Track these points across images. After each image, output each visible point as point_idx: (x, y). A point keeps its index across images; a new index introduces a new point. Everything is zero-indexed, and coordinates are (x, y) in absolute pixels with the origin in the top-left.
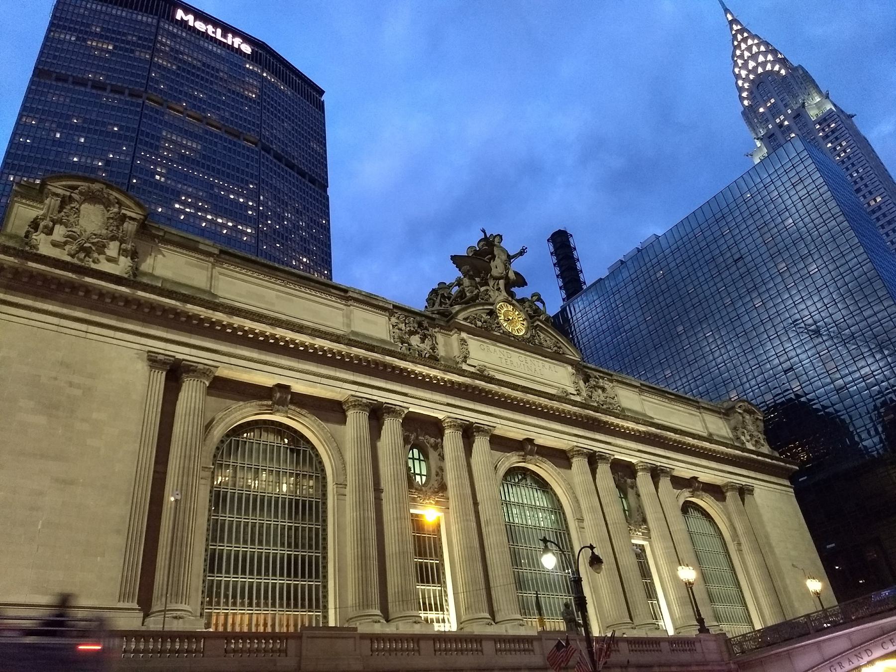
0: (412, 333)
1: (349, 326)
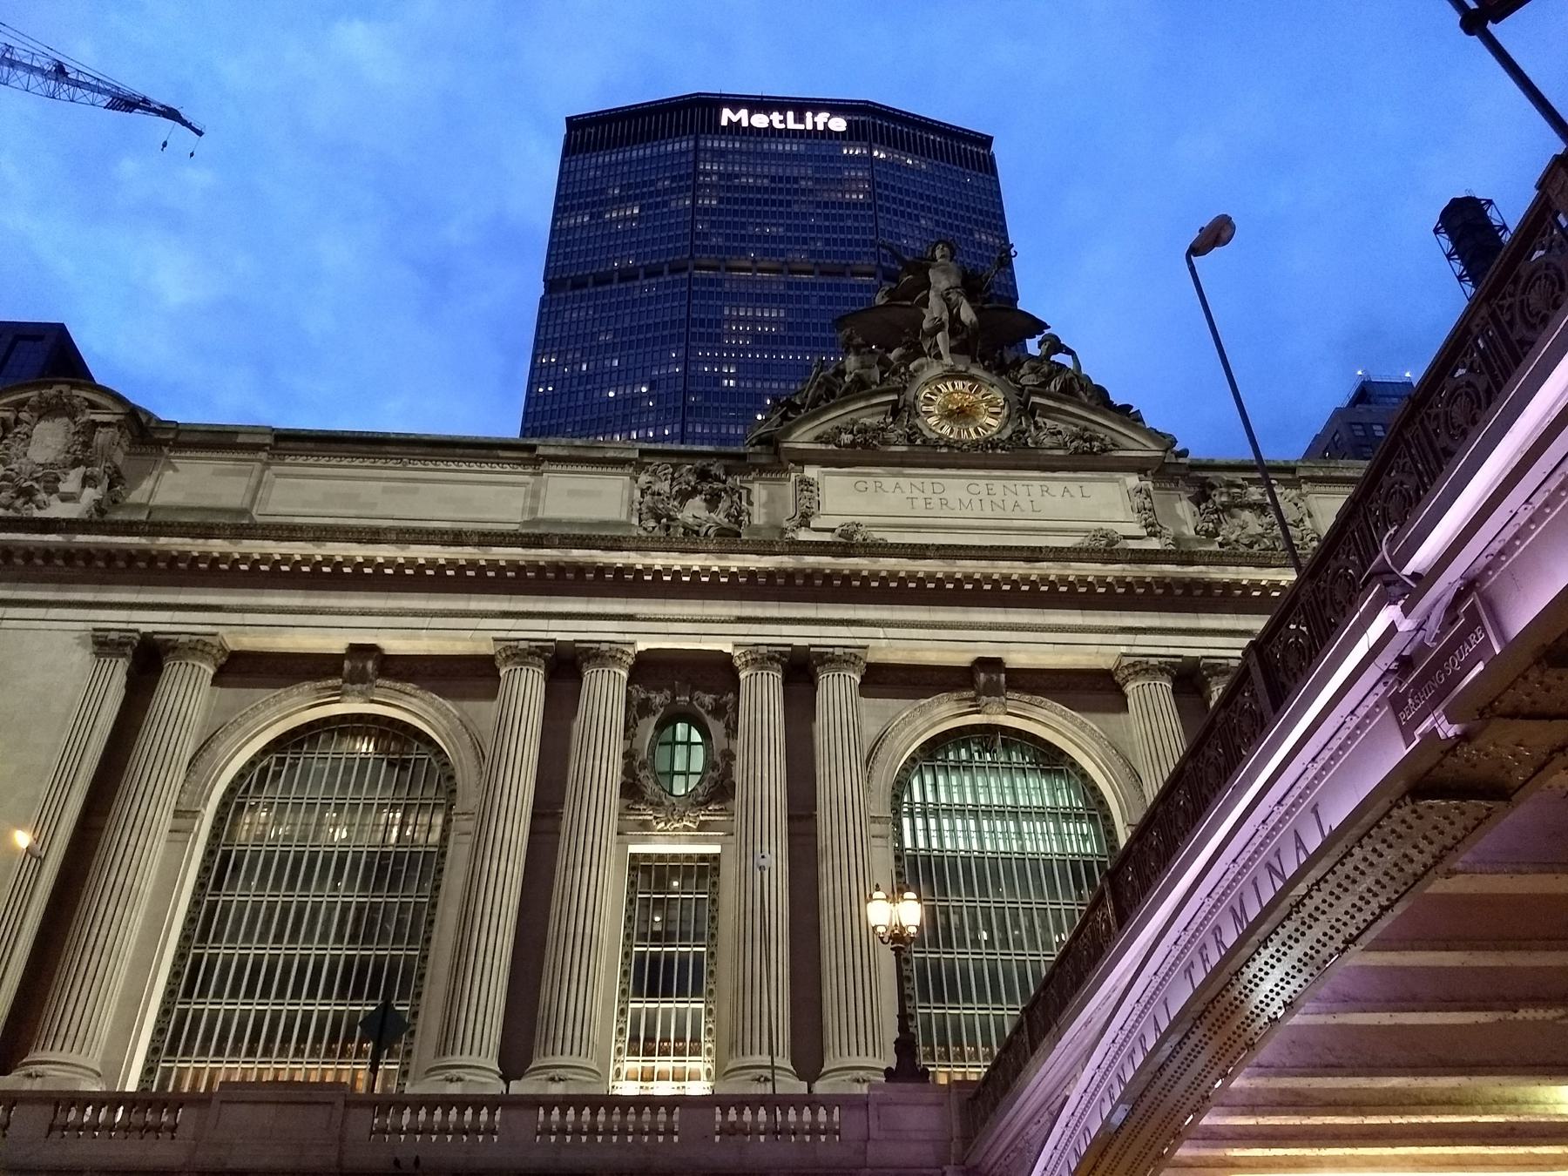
0: (685, 496)
1: (533, 510)
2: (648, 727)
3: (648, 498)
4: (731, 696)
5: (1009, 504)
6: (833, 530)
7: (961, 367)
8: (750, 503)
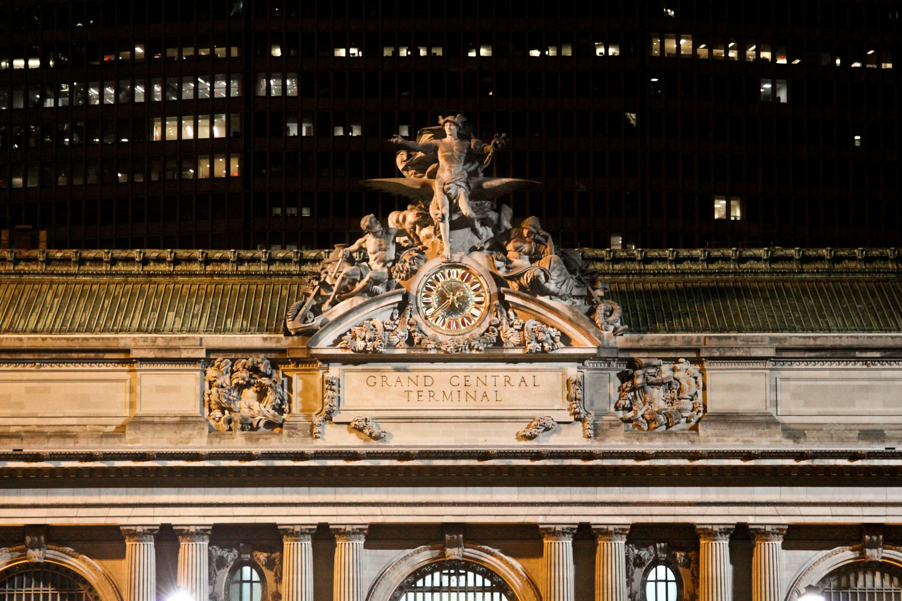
0: (240, 388)
1: (132, 405)
2: (224, 574)
3: (214, 390)
4: (278, 554)
5: (479, 395)
6: (349, 423)
7: (456, 258)
8: (290, 390)
